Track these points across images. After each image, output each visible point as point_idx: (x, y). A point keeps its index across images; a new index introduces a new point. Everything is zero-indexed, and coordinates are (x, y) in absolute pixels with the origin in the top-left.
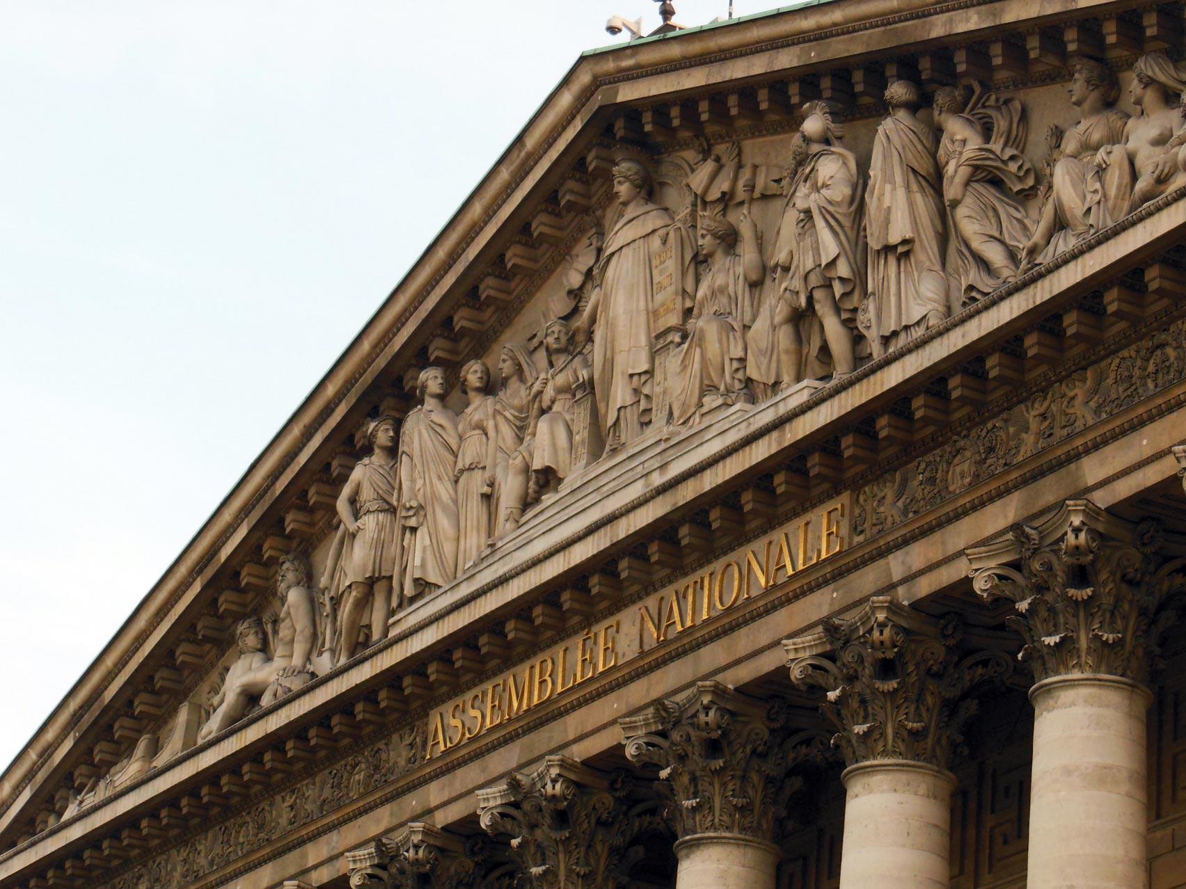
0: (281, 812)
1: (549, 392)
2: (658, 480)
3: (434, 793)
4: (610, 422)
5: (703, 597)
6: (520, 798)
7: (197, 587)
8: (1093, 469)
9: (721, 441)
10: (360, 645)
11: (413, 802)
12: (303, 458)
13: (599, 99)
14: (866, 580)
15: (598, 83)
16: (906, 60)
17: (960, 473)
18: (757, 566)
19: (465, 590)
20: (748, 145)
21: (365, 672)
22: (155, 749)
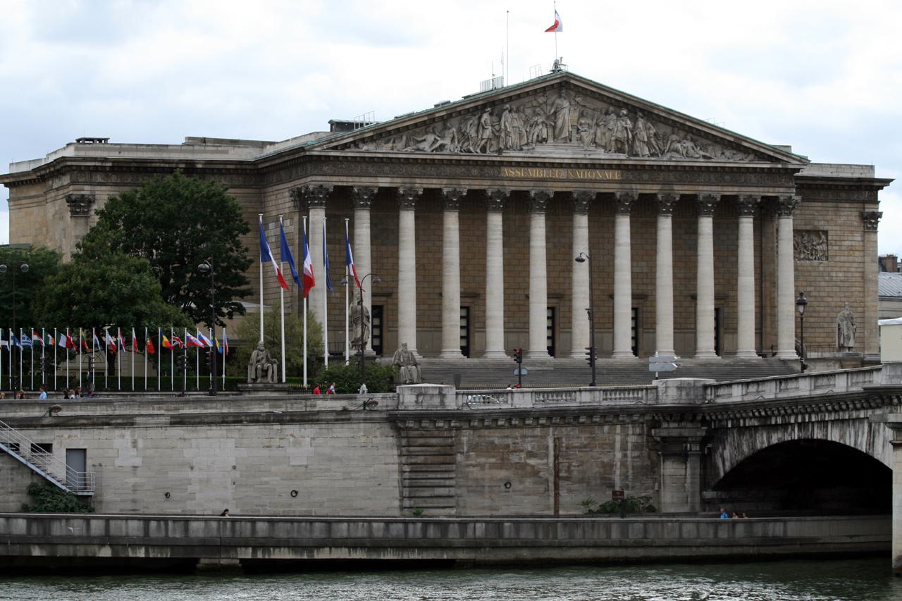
0: (448, 170)
1: (540, 121)
2: (588, 157)
3: (506, 183)
4: (563, 136)
5: (586, 174)
6: (542, 194)
7: (426, 118)
8: (676, 187)
9: (601, 155)
10: (484, 149)
11: (499, 183)
12: (467, 107)
13: (565, 79)
14: (627, 186)
15: (566, 76)
16: (642, 110)
17: (645, 176)
18: (599, 174)
19: (529, 155)
20: (588, 98)
21: (498, 159)
22: (394, 142)
